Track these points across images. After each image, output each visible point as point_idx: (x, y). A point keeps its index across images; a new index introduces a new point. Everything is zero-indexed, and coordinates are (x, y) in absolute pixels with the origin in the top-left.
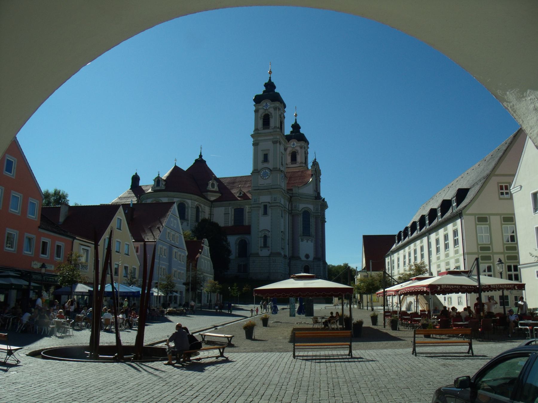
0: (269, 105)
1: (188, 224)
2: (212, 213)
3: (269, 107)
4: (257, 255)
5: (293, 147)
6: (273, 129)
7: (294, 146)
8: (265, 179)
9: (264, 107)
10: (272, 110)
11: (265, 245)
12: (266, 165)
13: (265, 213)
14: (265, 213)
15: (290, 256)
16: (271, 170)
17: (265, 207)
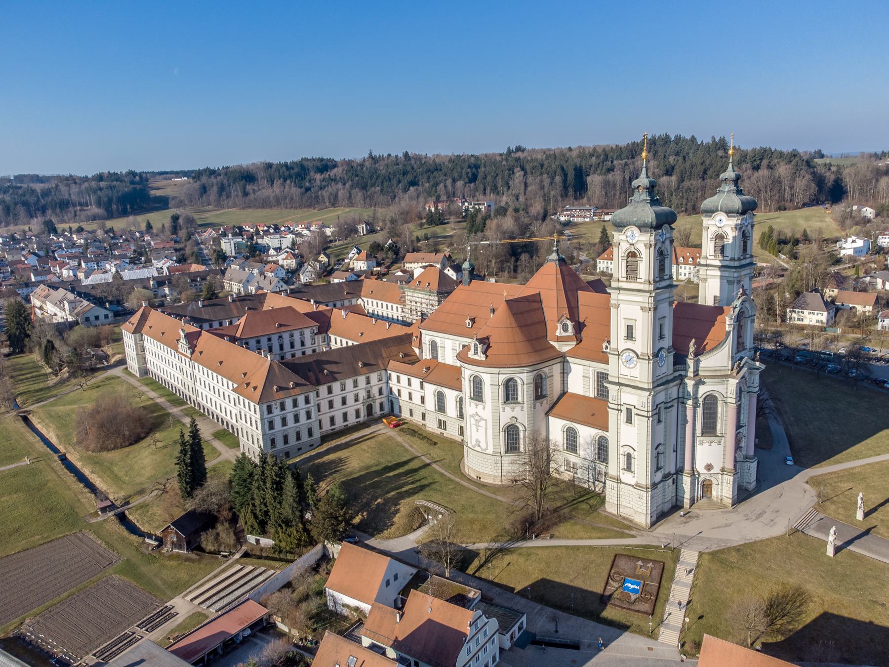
0: (637, 235)
1: (522, 408)
2: (565, 371)
3: (636, 239)
4: (619, 481)
5: (719, 225)
6: (641, 283)
7: (722, 225)
8: (629, 368)
9: (628, 239)
10: (641, 247)
11: (629, 468)
12: (629, 344)
13: (629, 420)
14: (629, 420)
15: (678, 466)
16: (637, 356)
17: (629, 411)
